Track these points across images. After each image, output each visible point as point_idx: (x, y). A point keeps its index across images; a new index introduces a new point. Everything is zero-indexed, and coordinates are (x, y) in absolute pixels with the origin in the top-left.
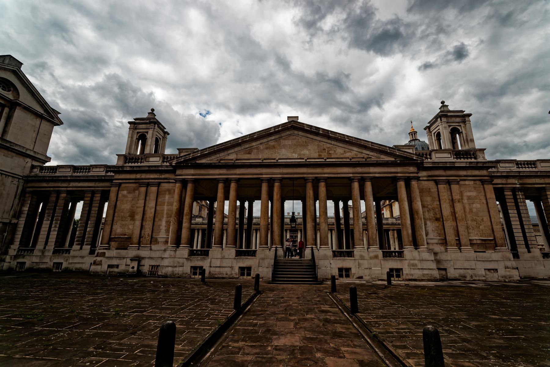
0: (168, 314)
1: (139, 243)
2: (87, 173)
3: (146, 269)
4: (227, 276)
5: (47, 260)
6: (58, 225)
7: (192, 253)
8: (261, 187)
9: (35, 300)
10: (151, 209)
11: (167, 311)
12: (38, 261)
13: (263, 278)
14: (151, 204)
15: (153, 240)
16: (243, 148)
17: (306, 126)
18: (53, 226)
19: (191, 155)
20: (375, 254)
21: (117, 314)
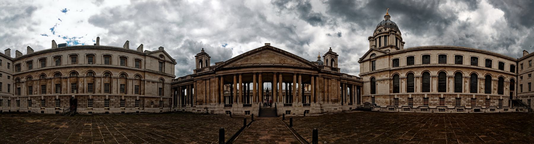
1: (206, 102)
3: (209, 112)
7: (226, 106)
8: (253, 77)
10: (208, 89)
14: (208, 87)
20: (301, 105)
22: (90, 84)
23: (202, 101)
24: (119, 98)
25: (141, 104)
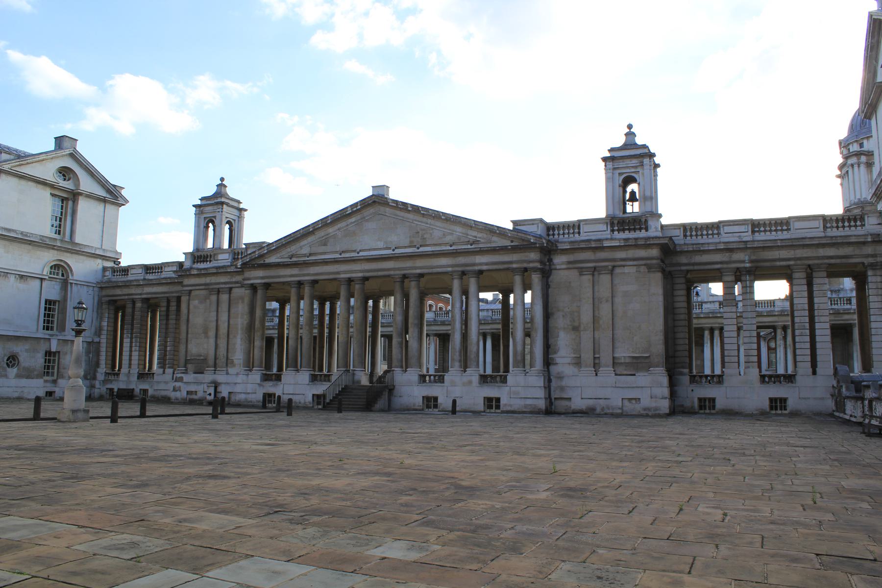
1: (215, 366)
15: (228, 362)
23: (205, 360)
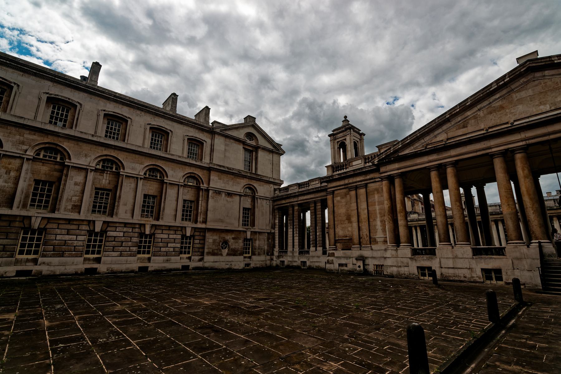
0: (406, 315)
1: (360, 243)
2: (307, 187)
4: (465, 279)
5: (296, 259)
6: (298, 232)
7: (415, 252)
8: (492, 164)
9: (298, 290)
10: (363, 210)
11: (404, 312)
12: (291, 260)
13: (524, 284)
14: (363, 206)
15: (372, 241)
16: (453, 123)
17: (557, 58)
18: (295, 232)
19: (392, 149)
21: (358, 308)
22: (44, 183)
23: (351, 240)
24: (137, 230)
25: (198, 246)
